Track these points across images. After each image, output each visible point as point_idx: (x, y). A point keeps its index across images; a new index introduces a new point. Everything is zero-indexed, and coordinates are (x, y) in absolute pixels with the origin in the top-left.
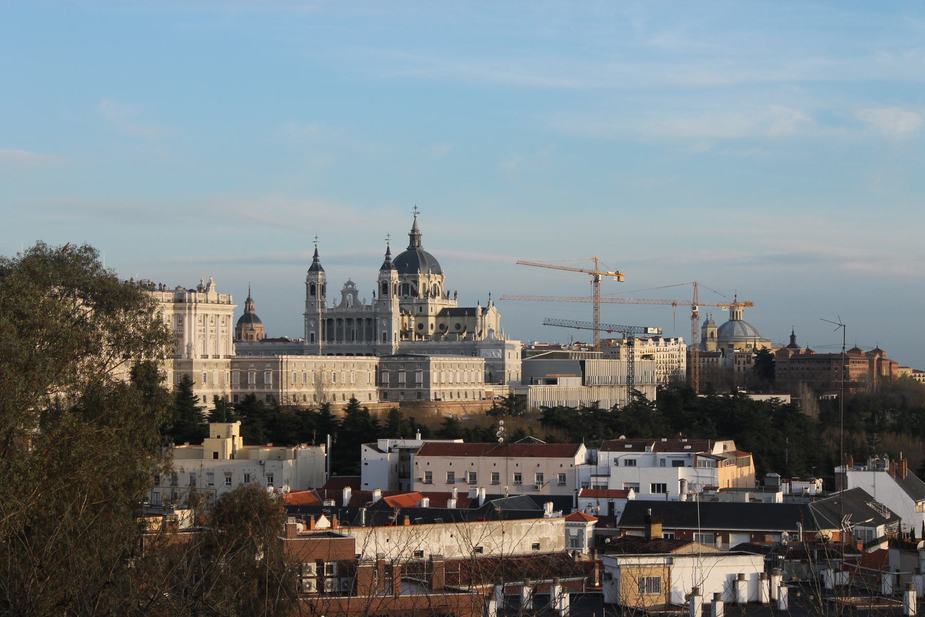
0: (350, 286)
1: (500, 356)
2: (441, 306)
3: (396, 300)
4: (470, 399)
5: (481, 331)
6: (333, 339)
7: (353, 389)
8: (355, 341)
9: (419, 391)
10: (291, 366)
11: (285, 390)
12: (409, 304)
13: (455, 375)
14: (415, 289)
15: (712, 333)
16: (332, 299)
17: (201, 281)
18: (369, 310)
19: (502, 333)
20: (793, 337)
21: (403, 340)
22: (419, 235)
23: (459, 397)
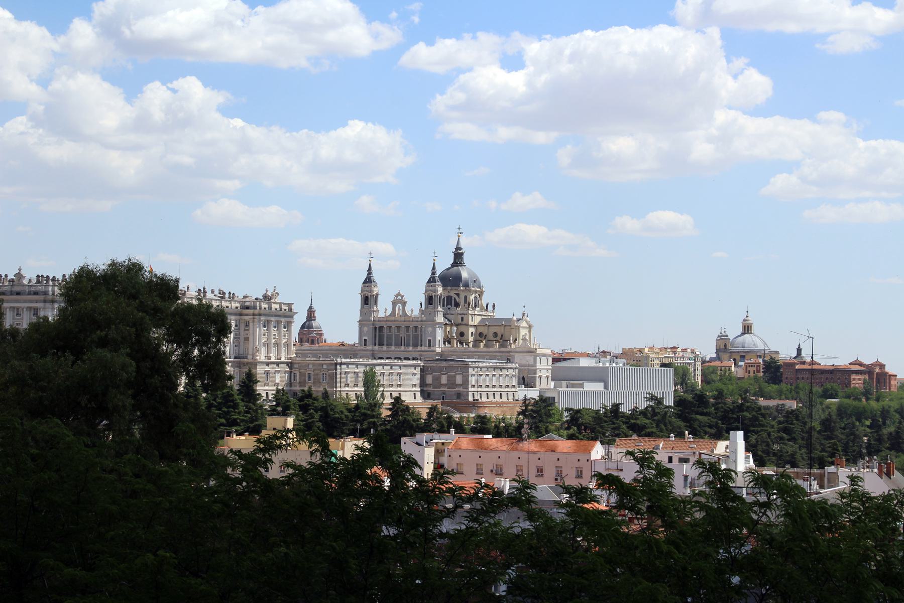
0: (399, 297)
4: (504, 399)
5: (516, 340)
6: (383, 345)
7: (399, 389)
8: (403, 346)
9: (458, 392)
12: (452, 314)
14: (457, 300)
15: (725, 345)
16: (383, 309)
17: (267, 291)
19: (535, 341)
20: (799, 350)
21: (446, 345)
22: (462, 254)
23: (494, 398)
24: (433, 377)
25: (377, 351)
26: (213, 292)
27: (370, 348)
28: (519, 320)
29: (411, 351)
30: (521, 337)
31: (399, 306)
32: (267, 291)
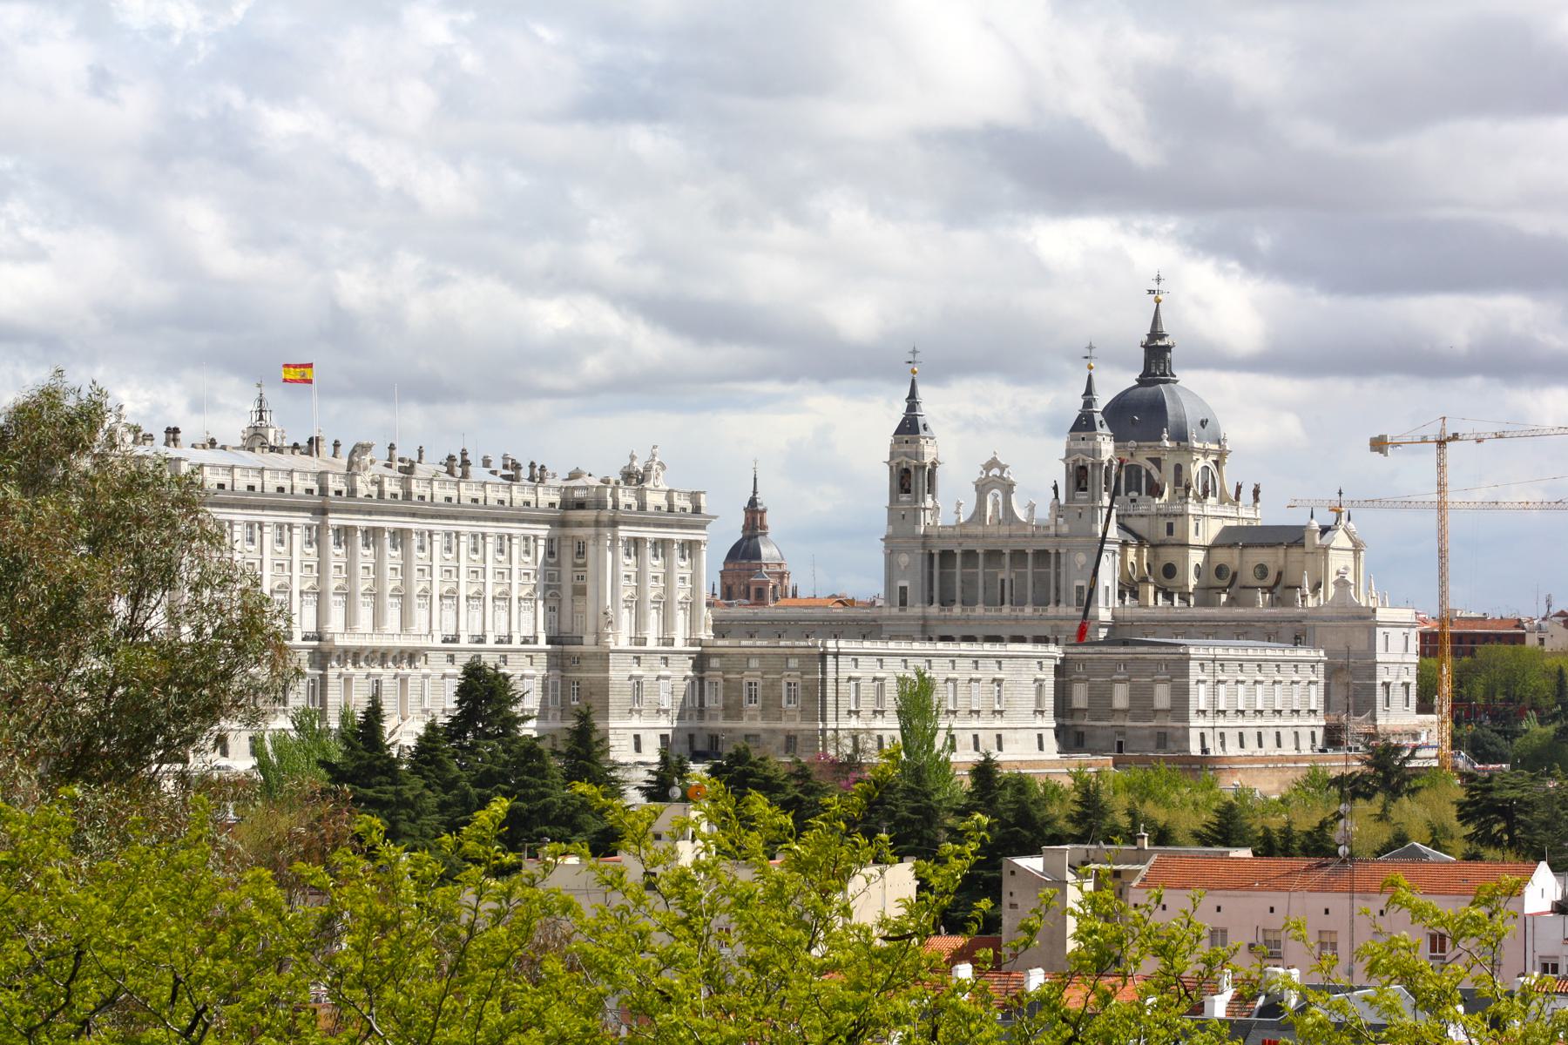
0: (995, 471)
1: (1364, 646)
2: (1219, 521)
4: (1288, 749)
5: (1319, 585)
6: (953, 601)
7: (998, 723)
9: (1162, 730)
11: (831, 725)
12: (1142, 516)
17: (633, 458)
18: (1042, 532)
19: (1370, 588)
21: (1127, 603)
22: (1168, 348)
23: (1260, 745)
24: (1091, 689)
25: (937, 619)
26: (486, 463)
27: (916, 610)
28: (1325, 530)
29: (1030, 619)
30: (1333, 577)
31: (996, 496)
32: (633, 458)
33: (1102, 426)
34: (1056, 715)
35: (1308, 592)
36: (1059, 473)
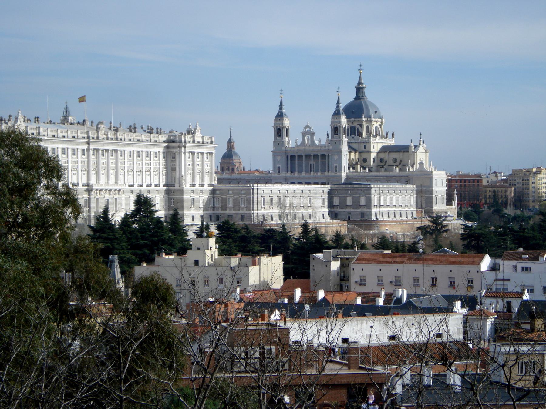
2: (381, 144)
3: (345, 140)
4: (404, 218)
5: (414, 164)
7: (310, 211)
8: (312, 172)
9: (363, 212)
10: (260, 193)
11: (256, 212)
13: (391, 199)
14: (360, 130)
17: (190, 126)
18: (323, 148)
19: (431, 165)
21: (351, 171)
22: (363, 88)
23: (395, 217)
27: (283, 174)
30: (418, 162)
33: (342, 113)
34: (328, 208)
35: (410, 166)
36: (329, 130)
